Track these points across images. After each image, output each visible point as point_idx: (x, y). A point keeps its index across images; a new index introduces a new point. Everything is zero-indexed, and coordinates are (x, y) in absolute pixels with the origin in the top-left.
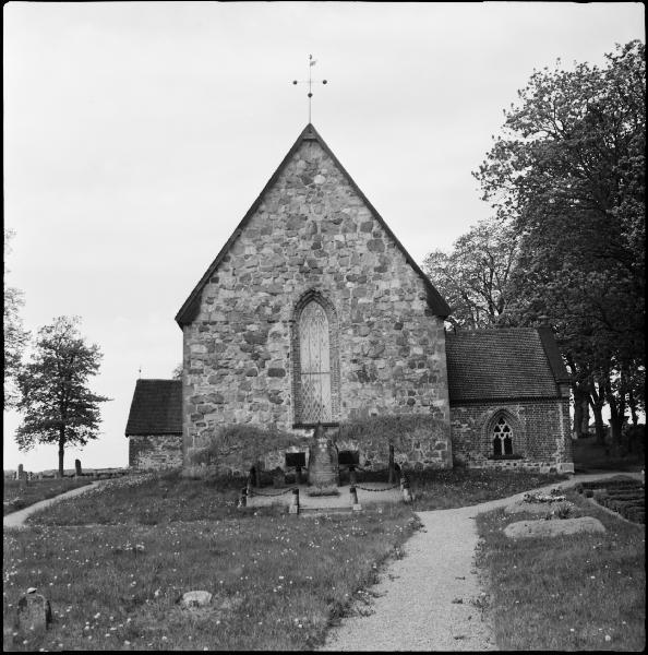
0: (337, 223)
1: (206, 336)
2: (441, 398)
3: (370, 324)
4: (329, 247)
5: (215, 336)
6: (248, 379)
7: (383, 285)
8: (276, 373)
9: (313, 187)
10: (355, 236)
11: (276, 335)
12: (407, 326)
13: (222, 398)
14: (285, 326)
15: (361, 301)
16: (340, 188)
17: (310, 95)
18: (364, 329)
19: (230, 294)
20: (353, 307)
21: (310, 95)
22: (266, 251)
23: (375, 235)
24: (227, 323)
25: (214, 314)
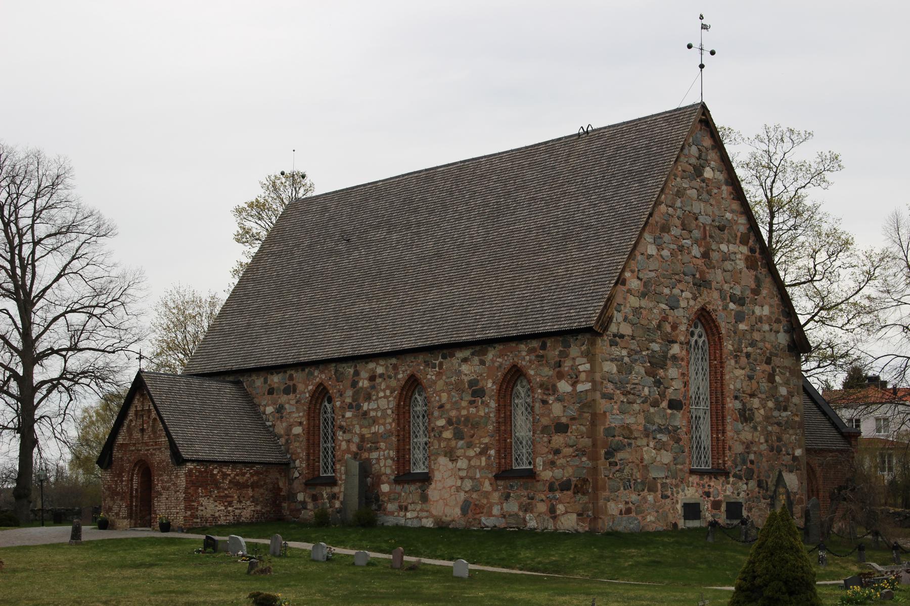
0: (721, 229)
1: (616, 351)
2: (800, 448)
3: (748, 355)
4: (715, 256)
5: (624, 353)
6: (652, 410)
7: (758, 310)
8: (675, 405)
9: (703, 181)
10: (732, 248)
11: (674, 358)
12: (776, 361)
13: (631, 432)
14: (682, 349)
15: (742, 327)
16: (724, 188)
17: (702, 66)
18: (744, 360)
19: (634, 301)
20: (735, 333)
21: (702, 66)
22: (666, 253)
23: (752, 250)
24: (633, 338)
25: (621, 325)
